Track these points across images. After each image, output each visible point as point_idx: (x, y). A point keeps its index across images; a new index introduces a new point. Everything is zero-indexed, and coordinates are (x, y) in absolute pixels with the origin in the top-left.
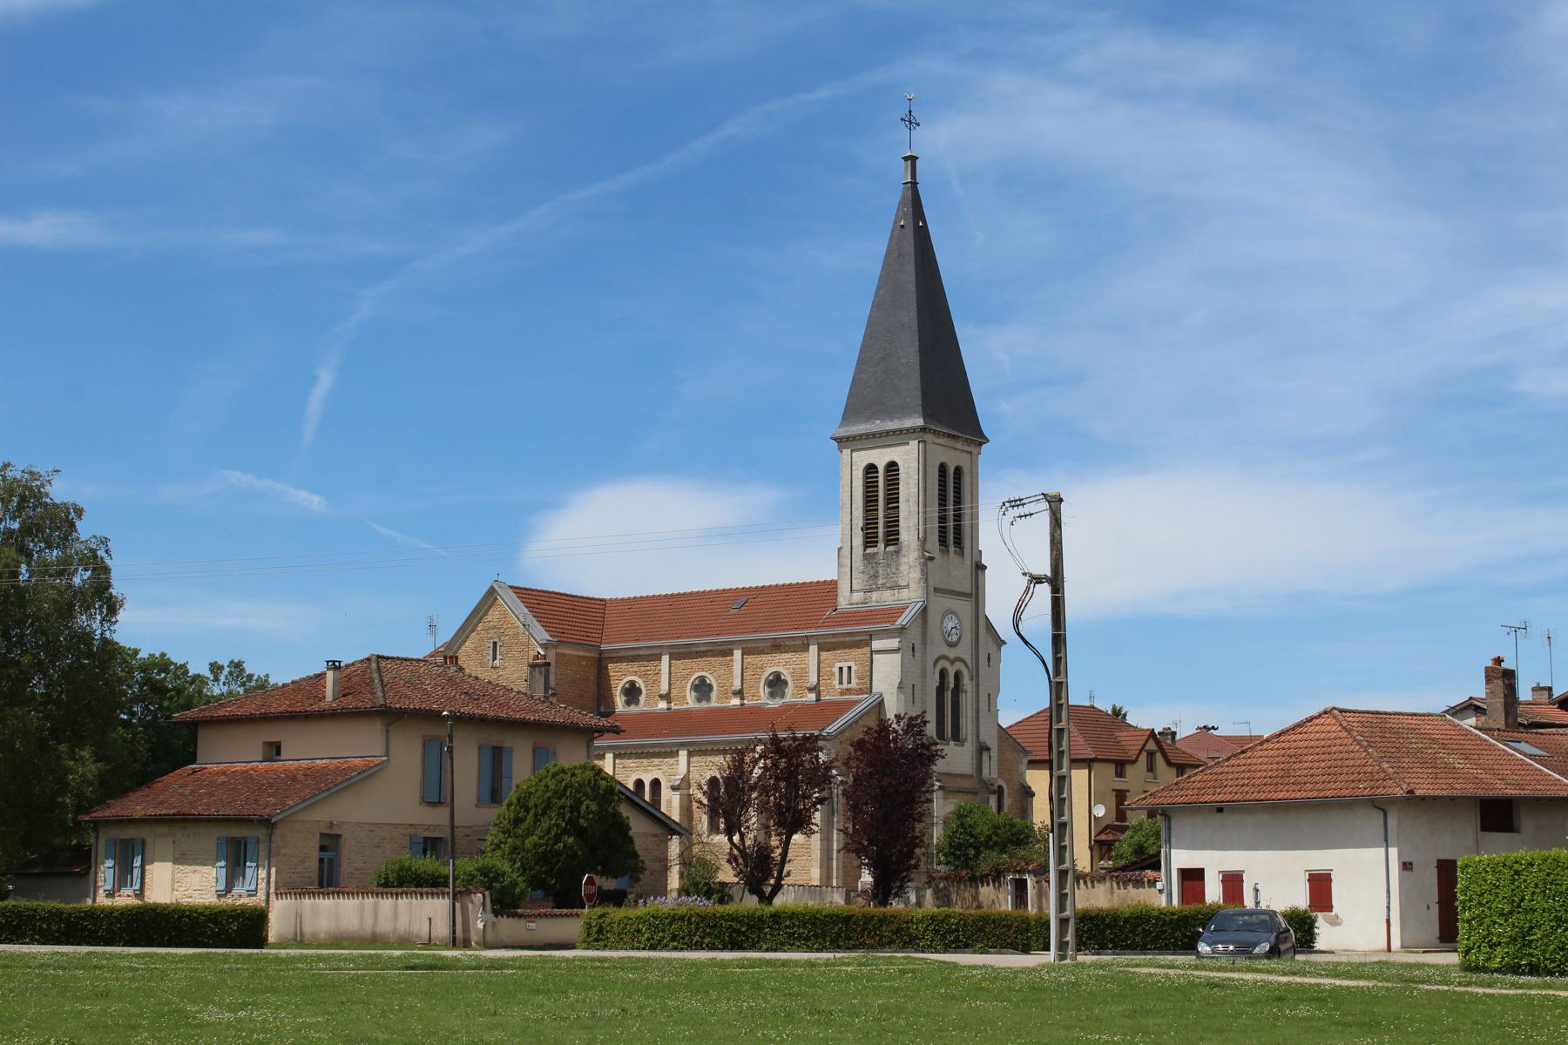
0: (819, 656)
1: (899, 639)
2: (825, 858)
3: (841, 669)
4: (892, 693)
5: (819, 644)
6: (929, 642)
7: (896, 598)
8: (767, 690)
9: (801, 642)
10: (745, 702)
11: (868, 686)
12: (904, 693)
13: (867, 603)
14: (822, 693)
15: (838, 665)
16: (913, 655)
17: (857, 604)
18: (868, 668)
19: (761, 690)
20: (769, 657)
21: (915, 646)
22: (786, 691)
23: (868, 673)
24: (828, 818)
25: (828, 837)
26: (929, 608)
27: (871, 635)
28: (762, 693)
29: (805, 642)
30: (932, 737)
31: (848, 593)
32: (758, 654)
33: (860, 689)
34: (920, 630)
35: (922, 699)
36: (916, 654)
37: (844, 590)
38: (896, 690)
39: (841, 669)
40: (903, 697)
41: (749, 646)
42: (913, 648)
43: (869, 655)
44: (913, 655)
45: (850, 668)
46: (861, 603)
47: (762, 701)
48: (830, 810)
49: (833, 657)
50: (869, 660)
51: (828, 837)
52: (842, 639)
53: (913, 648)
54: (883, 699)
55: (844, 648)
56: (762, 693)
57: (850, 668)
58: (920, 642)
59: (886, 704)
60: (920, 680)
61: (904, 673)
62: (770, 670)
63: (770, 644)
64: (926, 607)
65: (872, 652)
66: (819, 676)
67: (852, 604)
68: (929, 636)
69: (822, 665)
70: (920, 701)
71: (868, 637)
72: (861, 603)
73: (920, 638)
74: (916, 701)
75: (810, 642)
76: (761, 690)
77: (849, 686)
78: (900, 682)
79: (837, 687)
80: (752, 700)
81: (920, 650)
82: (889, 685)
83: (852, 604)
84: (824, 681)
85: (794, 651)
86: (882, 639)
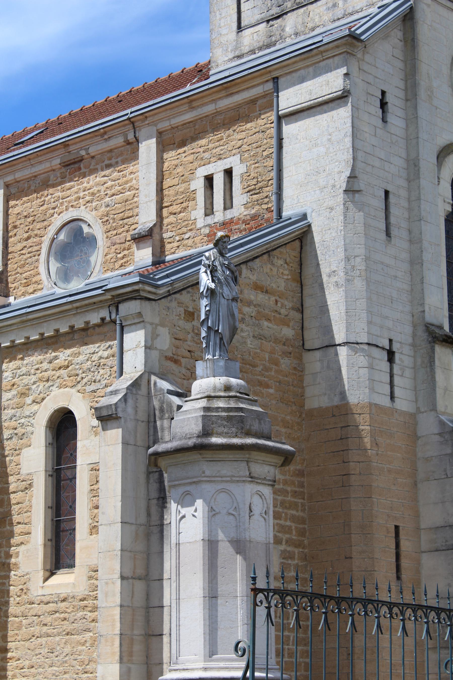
0: (160, 161)
1: (344, 70)
2: (138, 631)
3: (209, 180)
4: (332, 209)
5: (160, 134)
6: (422, 94)
7: (339, 12)
8: (54, 265)
9: (120, 141)
10: (11, 299)
11: (273, 205)
12: (360, 207)
13: (275, 45)
14: (168, 247)
15: (202, 172)
16: (384, 120)
17: (253, 52)
18: (272, 162)
19: (42, 269)
20: (57, 192)
21: (389, 98)
22: (93, 259)
23: (273, 174)
24: (149, 515)
25: (147, 567)
26: (419, 15)
27: (276, 80)
28: (43, 276)
29: (131, 137)
30: (441, 327)
31: (233, 35)
32: (35, 191)
33: (254, 217)
34: (400, 65)
35: (410, 232)
36: (390, 118)
37: (224, 31)
38: (341, 197)
39: (209, 180)
40: (359, 216)
41: (19, 175)
42: (383, 105)
43: (273, 132)
44: (384, 120)
45: (229, 173)
46: (260, 49)
47: (45, 292)
48: (154, 494)
49: (191, 158)
50: (274, 142)
51: (147, 567)
52: (209, 109)
53: (383, 105)
54: (310, 226)
55: (215, 128)
56: (43, 276)
57: (229, 173)
58: (401, 94)
59: (317, 238)
60: (404, 183)
61: (360, 155)
62: (58, 221)
63: (57, 161)
64: (411, 8)
65: (279, 118)
66: (160, 208)
67: (239, 57)
68: (423, 84)
69: (166, 184)
70: (404, 234)
71: (270, 86)
72: (260, 49)
73: (401, 85)
74: (394, 231)
75: (141, 134)
76: (42, 269)
77: (229, 214)
78: (352, 177)
79: (200, 223)
80: (24, 294)
81: (400, 113)
82: (322, 189)
83: (239, 57)
84: (172, 219)
85: (108, 166)
86: (302, 80)
